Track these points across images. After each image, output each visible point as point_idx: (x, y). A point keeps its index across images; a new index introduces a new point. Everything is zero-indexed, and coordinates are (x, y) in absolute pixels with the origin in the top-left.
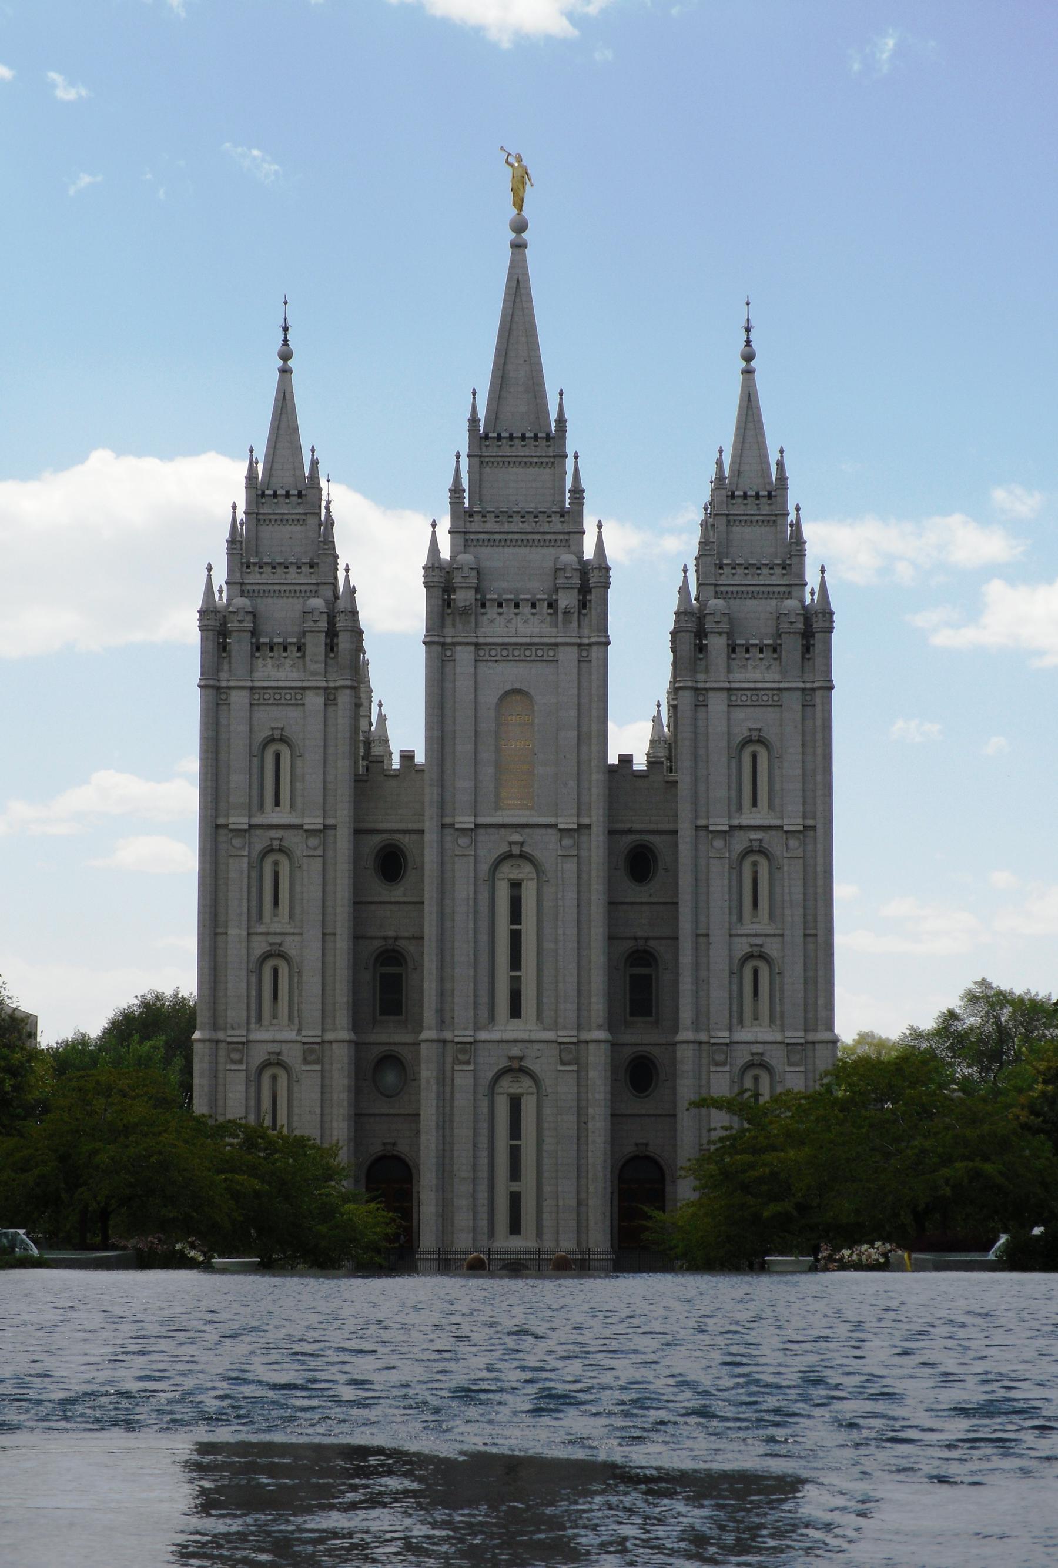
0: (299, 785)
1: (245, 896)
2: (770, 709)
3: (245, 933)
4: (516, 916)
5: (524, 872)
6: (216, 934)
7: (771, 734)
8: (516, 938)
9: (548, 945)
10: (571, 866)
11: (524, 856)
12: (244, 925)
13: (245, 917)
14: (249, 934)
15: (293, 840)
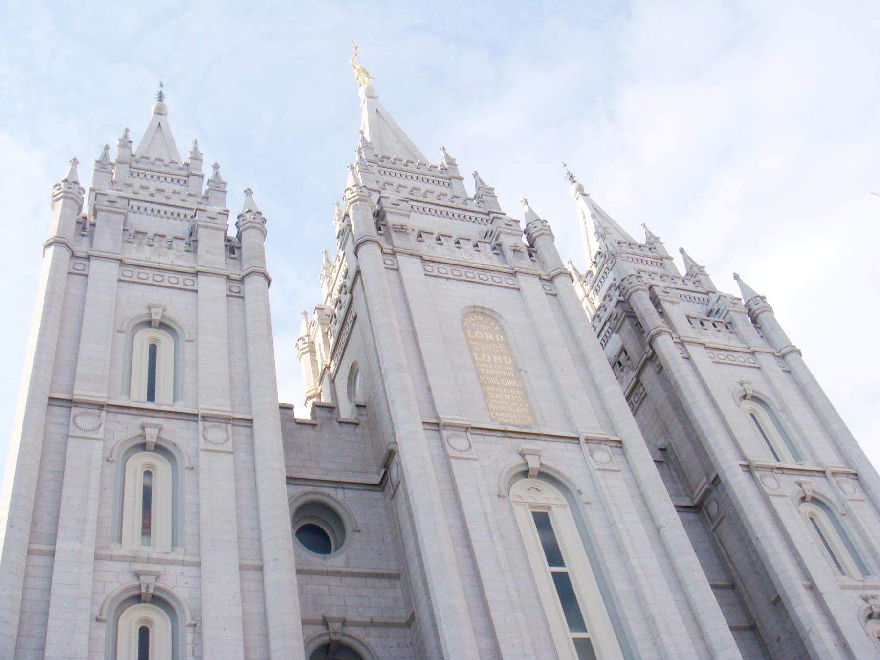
0: (188, 373)
1: (94, 494)
2: (751, 370)
3: (89, 550)
4: (554, 556)
5: (548, 496)
6: (30, 553)
7: (762, 389)
8: (563, 584)
9: (620, 585)
10: (616, 486)
11: (545, 475)
12: (90, 536)
13: (91, 526)
14: (98, 558)
15: (175, 432)
